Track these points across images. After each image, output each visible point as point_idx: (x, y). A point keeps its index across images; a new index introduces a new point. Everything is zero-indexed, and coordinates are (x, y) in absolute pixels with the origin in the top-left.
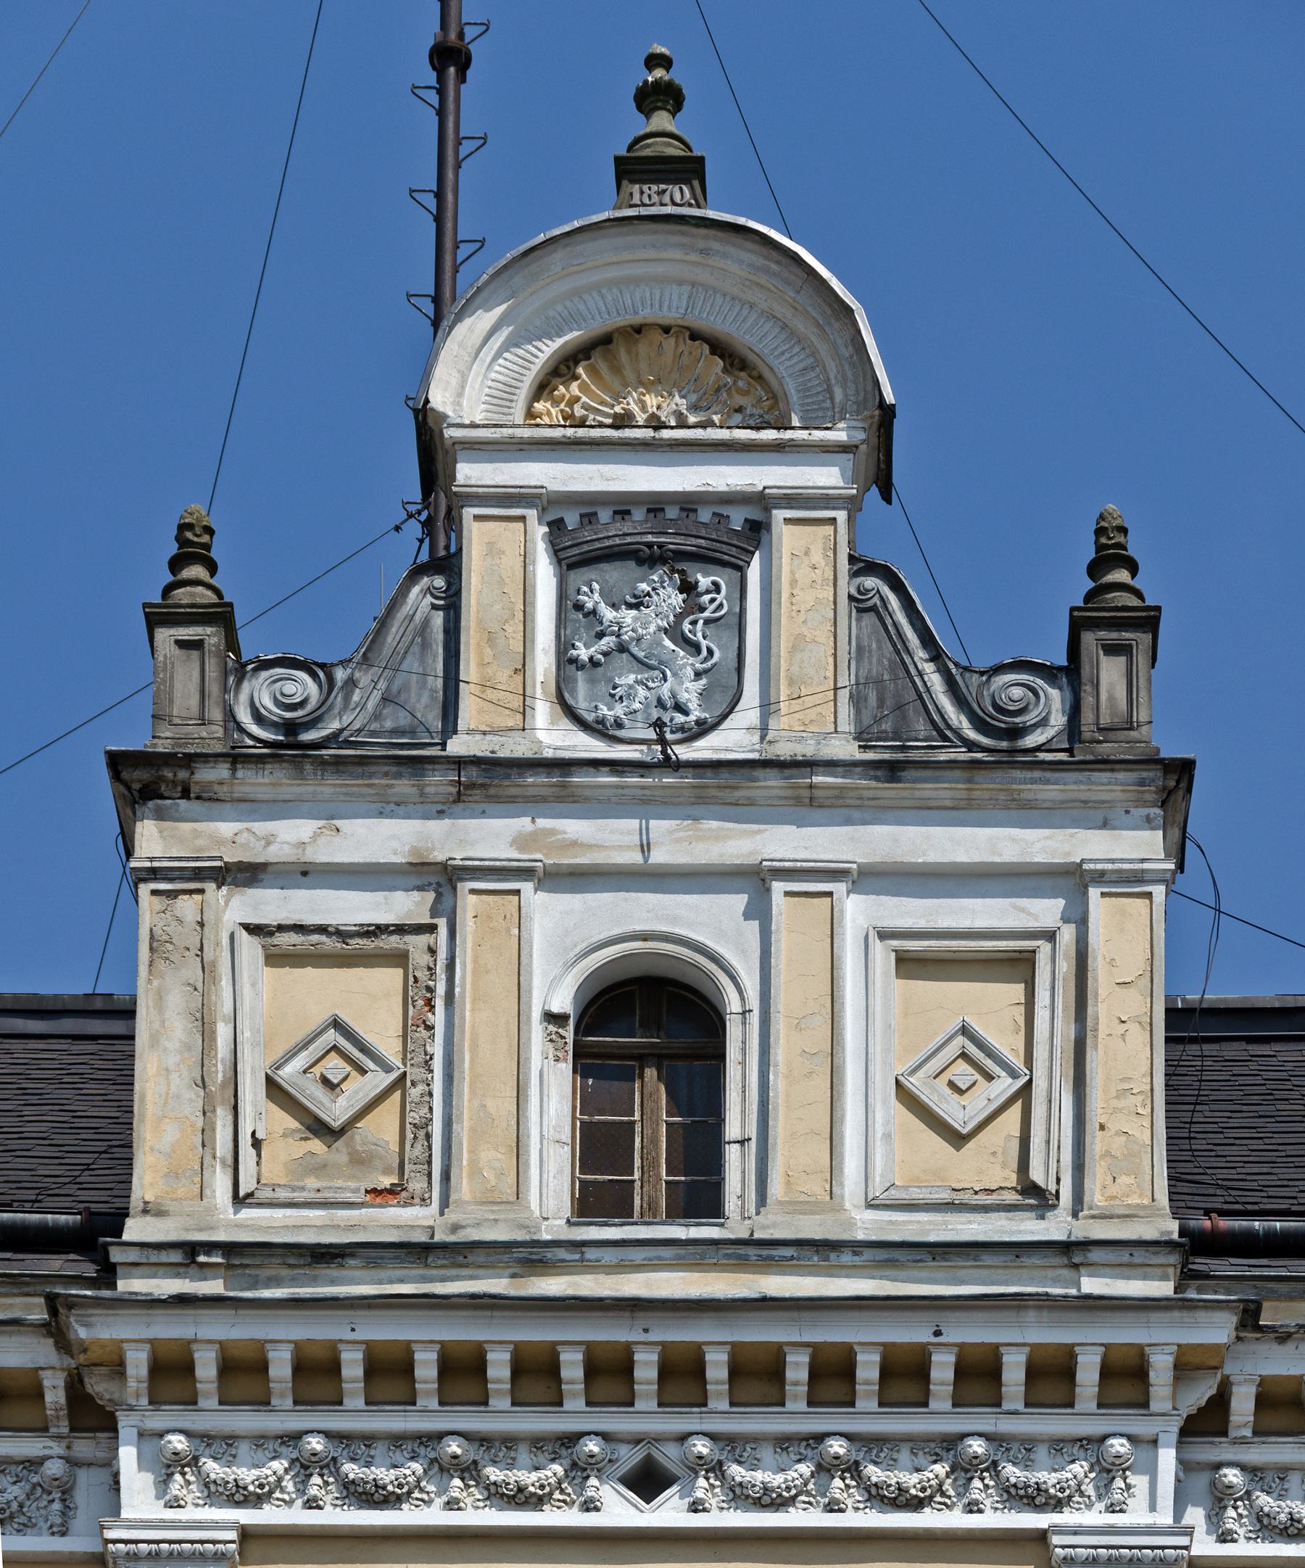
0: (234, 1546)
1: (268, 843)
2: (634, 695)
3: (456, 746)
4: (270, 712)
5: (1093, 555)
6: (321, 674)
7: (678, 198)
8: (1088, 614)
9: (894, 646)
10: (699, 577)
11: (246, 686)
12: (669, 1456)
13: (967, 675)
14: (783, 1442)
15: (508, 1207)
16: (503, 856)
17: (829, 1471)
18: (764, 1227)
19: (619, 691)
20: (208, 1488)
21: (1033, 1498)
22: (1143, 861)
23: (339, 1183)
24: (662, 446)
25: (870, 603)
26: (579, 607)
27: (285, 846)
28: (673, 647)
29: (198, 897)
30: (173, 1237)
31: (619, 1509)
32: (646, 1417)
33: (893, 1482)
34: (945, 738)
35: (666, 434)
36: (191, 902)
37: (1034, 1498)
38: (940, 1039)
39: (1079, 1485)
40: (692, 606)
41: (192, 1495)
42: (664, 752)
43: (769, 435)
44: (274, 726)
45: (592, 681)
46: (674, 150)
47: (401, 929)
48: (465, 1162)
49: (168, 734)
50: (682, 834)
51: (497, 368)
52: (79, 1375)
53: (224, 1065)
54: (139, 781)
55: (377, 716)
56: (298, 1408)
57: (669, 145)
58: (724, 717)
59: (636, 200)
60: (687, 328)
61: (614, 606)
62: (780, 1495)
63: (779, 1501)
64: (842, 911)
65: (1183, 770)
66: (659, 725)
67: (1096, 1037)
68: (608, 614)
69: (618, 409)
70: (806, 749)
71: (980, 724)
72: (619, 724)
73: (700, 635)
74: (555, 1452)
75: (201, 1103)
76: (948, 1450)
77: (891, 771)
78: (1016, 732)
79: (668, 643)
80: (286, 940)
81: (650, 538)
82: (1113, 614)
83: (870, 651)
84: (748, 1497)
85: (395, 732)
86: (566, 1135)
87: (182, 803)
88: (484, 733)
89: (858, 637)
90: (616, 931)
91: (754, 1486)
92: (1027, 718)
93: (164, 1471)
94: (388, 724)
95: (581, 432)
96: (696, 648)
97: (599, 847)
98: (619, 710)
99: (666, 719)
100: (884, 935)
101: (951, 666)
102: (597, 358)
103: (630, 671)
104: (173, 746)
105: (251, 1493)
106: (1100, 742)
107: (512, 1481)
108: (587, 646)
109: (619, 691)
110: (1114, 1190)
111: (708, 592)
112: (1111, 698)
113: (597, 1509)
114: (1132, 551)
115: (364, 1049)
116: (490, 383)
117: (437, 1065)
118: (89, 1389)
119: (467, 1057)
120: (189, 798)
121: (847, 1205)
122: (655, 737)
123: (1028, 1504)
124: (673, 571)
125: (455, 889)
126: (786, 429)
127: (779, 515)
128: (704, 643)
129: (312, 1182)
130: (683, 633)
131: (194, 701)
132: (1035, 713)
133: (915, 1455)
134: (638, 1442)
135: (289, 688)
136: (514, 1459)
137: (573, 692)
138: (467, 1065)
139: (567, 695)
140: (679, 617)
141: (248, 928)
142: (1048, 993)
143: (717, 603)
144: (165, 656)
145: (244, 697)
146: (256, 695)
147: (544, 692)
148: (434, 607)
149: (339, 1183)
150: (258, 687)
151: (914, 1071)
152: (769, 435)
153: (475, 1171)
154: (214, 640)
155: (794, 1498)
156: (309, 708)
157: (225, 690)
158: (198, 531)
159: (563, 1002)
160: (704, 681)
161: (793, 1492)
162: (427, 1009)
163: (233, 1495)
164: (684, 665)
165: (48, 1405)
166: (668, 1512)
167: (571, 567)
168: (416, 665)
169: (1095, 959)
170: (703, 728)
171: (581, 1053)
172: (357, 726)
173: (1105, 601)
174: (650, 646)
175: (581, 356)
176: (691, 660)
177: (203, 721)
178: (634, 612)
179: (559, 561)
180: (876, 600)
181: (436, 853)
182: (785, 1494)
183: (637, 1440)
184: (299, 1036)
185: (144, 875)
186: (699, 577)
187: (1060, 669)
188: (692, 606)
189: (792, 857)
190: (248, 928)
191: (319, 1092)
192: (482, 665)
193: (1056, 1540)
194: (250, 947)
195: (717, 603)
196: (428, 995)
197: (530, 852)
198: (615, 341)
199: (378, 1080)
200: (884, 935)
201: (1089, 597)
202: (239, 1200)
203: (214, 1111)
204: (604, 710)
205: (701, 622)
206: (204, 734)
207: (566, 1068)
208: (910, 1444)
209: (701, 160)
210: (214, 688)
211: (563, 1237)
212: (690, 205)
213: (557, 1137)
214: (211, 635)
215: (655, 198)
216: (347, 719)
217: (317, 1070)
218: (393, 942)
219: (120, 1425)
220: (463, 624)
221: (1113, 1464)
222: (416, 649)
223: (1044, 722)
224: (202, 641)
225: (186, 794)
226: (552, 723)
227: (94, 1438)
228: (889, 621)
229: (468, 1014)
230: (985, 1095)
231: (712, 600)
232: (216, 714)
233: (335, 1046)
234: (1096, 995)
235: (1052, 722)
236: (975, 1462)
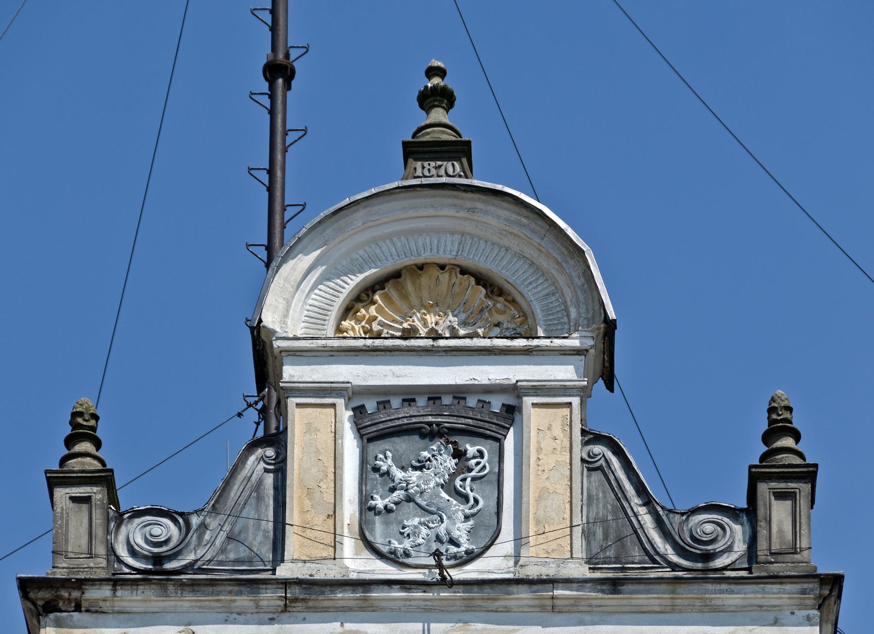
2: (418, 533)
4: (142, 548)
6: (181, 520)
7: (450, 171)
9: (616, 495)
10: (468, 446)
11: (123, 530)
19: (407, 531)
24: (439, 352)
25: (597, 464)
26: (376, 469)
28: (448, 498)
34: (654, 561)
40: (463, 468)
42: (441, 574)
43: (521, 343)
44: (145, 558)
51: (314, 296)
54: (43, 599)
55: (223, 550)
58: (487, 548)
59: (419, 172)
60: (458, 266)
61: (403, 468)
65: (835, 582)
68: (398, 474)
69: (406, 325)
70: (550, 571)
73: (468, 489)
77: (614, 585)
78: (708, 557)
79: (444, 495)
82: (781, 468)
83: (598, 499)
85: (237, 561)
87: (76, 615)
88: (305, 561)
89: (588, 489)
94: (232, 556)
101: (659, 509)
103: (415, 516)
104: (68, 574)
108: (382, 498)
111: (474, 457)
112: (780, 531)
116: (308, 307)
120: (80, 611)
126: (533, 338)
127: (528, 401)
128: (471, 495)
130: (455, 488)
131: (84, 541)
132: (723, 542)
135: (156, 530)
137: (372, 531)
139: (367, 534)
140: (453, 476)
143: (481, 465)
145: (122, 537)
146: (131, 536)
152: (521, 343)
156: (171, 545)
157: (108, 532)
158: (87, 417)
160: (471, 522)
167: (370, 440)
170: (471, 557)
172: (208, 557)
173: (775, 460)
174: (431, 497)
175: (377, 287)
176: (462, 507)
177: (91, 555)
178: (418, 473)
179: (361, 437)
180: (602, 462)
186: (468, 446)
188: (463, 468)
192: (303, 512)
195: (481, 465)
198: (403, 276)
204: (395, 544)
205: (469, 479)
206: (92, 565)
210: (99, 532)
212: (460, 176)
215: (434, 172)
216: (200, 552)
222: (252, 501)
223: (729, 549)
225: (78, 608)
226: (356, 554)
228: (612, 478)
232: (101, 550)
235: (736, 548)
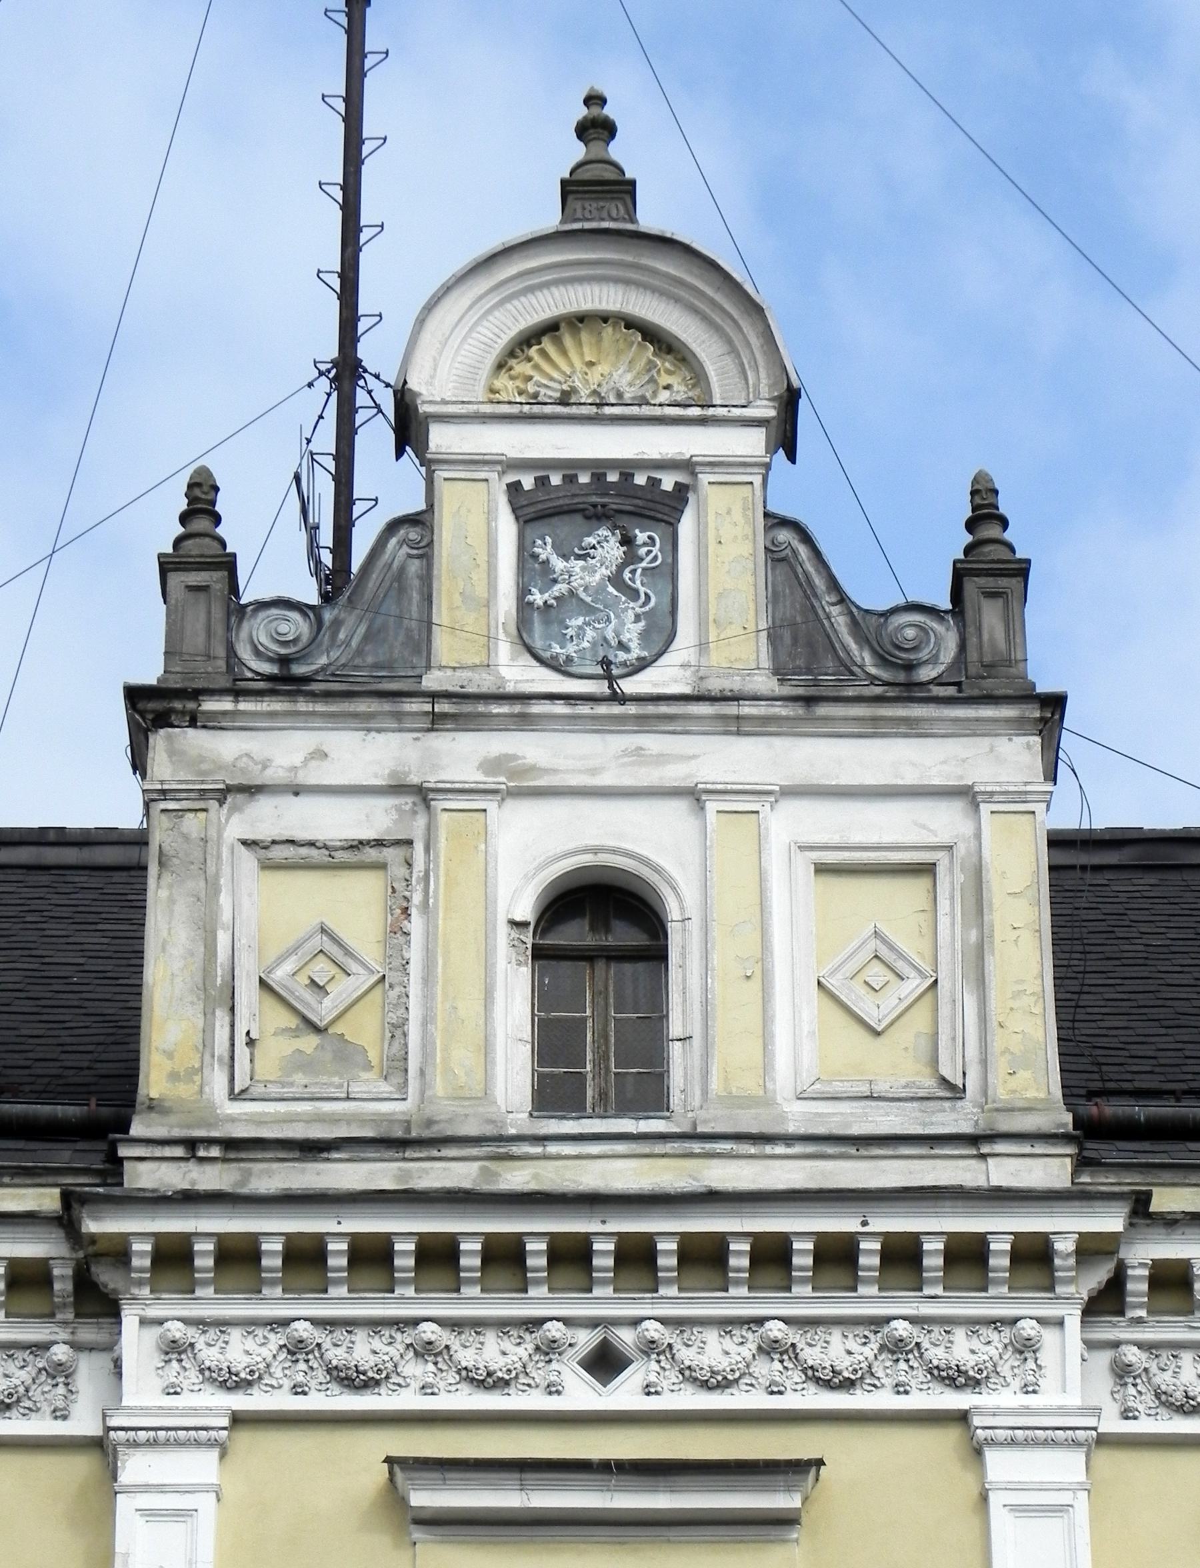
0: (226, 1433)
1: (265, 767)
2: (580, 637)
3: (431, 682)
4: (266, 648)
5: (970, 514)
6: (312, 616)
7: (614, 213)
8: (969, 566)
9: (805, 592)
10: (637, 531)
11: (246, 625)
12: (626, 1337)
13: (868, 617)
14: (726, 1324)
15: (477, 1102)
16: (472, 779)
17: (768, 1353)
18: (705, 1122)
19: (570, 632)
20: (203, 1374)
21: (955, 1378)
22: (1026, 783)
23: (325, 1079)
24: (603, 420)
25: (783, 554)
26: (535, 557)
27: (280, 770)
28: (616, 593)
29: (202, 815)
30: (177, 1133)
31: (581, 1393)
32: (604, 1302)
33: (827, 1365)
34: (852, 673)
35: (608, 410)
36: (196, 820)
37: (954, 1379)
38: (855, 943)
39: (995, 1366)
40: (631, 558)
41: (188, 1381)
42: (611, 686)
43: (695, 412)
44: (270, 660)
45: (547, 623)
46: (610, 175)
47: (379, 843)
48: (438, 1060)
49: (178, 669)
50: (626, 760)
51: (463, 352)
52: (87, 1263)
53: (223, 970)
54: (153, 711)
55: (359, 652)
56: (287, 1296)
57: (606, 170)
58: (660, 655)
59: (579, 215)
60: (623, 319)
61: (565, 557)
62: (725, 1378)
63: (724, 1382)
64: (767, 829)
65: (1056, 703)
66: (606, 663)
67: (992, 943)
68: (558, 564)
69: (565, 387)
70: (734, 684)
71: (883, 660)
72: (569, 660)
73: (638, 582)
74: (520, 1337)
75: (202, 1006)
76: (876, 1333)
77: (809, 701)
78: (910, 667)
79: (611, 589)
80: (278, 853)
81: (595, 499)
82: (990, 568)
83: (784, 596)
84: (696, 1379)
85: (376, 666)
86: (527, 1034)
87: (190, 731)
88: (454, 668)
89: (773, 585)
90: (571, 846)
91: (702, 1369)
92: (921, 655)
93: (163, 1357)
94: (370, 660)
95: (536, 409)
96: (633, 594)
97: (555, 771)
98: (571, 649)
99: (611, 658)
100: (802, 848)
101: (854, 610)
102: (547, 344)
103: (580, 614)
104: (183, 680)
105: (242, 1380)
106: (984, 678)
107: (481, 1366)
108: (541, 592)
109: (570, 632)
110: (1013, 1083)
111: (645, 544)
112: (992, 639)
113: (558, 1393)
114: (1003, 510)
115: (348, 952)
116: (457, 365)
117: (415, 969)
118: (94, 1278)
119: (440, 962)
120: (195, 727)
121: (779, 1100)
122: (602, 672)
123: (949, 1385)
124: (616, 527)
125: (428, 807)
126: (709, 406)
127: (704, 478)
128: (642, 590)
129: (300, 1078)
130: (624, 581)
131: (201, 640)
132: (926, 651)
133: (846, 1337)
134: (596, 1326)
135: (284, 628)
136: (482, 1343)
137: (530, 632)
138: (440, 970)
139: (525, 636)
140: (621, 568)
141: (244, 843)
142: (948, 902)
143: (652, 555)
144: (177, 600)
145: (244, 634)
146: (254, 633)
147: (505, 631)
148: (410, 556)
149: (325, 1079)
150: (256, 626)
151: (833, 972)
152: (695, 412)
153: (448, 1070)
154: (219, 586)
155: (737, 1381)
156: (300, 645)
157: (228, 629)
158: (205, 489)
159: (526, 910)
160: (642, 623)
161: (737, 1375)
162: (403, 917)
163: (225, 1381)
164: (626, 609)
165: (56, 1293)
166: (624, 1394)
167: (526, 522)
168: (394, 607)
169: (988, 871)
170: (642, 665)
171: (539, 954)
172: (343, 661)
173: (983, 554)
174: (597, 592)
175: (533, 341)
176: (632, 605)
177: (209, 657)
178: (581, 563)
179: (517, 518)
180: (788, 551)
181: (412, 776)
182: (730, 1377)
183: (593, 1323)
184: (290, 942)
185: (155, 796)
186: (637, 531)
187: (946, 612)
188: (631, 558)
189: (722, 780)
190: (244, 843)
191: (308, 996)
192: (451, 609)
193: (977, 1421)
194: (248, 860)
195: (652, 555)
196: (405, 904)
197: (495, 775)
198: (562, 330)
199: (361, 981)
200: (802, 848)
201: (968, 550)
202: (234, 1096)
203: (214, 1013)
204: (557, 649)
205: (639, 571)
206: (210, 670)
207: (526, 971)
208: (842, 1327)
209: (633, 183)
210: (219, 629)
211: (528, 1131)
212: (624, 220)
213: (520, 1036)
214: (214, 579)
215: (595, 213)
216: (334, 654)
217: (307, 971)
218: (372, 854)
219: (123, 1314)
220: (435, 572)
221: (1025, 1346)
222: (393, 593)
223: (934, 660)
224: (208, 586)
225: (193, 724)
226: (512, 659)
227: (97, 1323)
228: (799, 570)
229: (440, 922)
230: (896, 995)
231: (650, 552)
232: (221, 651)
233: (321, 951)
234: (991, 904)
235: (942, 659)
236: (900, 1344)
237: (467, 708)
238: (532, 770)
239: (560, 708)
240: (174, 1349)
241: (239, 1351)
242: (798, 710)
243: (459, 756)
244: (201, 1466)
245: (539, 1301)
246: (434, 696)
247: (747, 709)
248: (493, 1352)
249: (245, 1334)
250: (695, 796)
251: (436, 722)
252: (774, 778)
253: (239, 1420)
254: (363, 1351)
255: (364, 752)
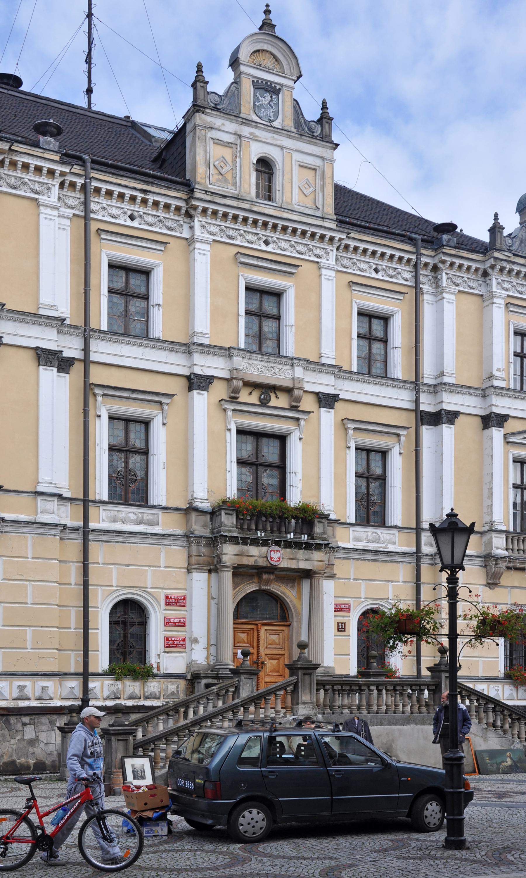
237: (248, 122)
238: (256, 136)
239: (262, 126)
240: (203, 226)
241: (212, 229)
242: (299, 136)
243: (246, 131)
244: (207, 247)
245: (258, 231)
246: (243, 119)
247: (292, 134)
248: (250, 237)
249: (215, 226)
250: (282, 148)
251: (243, 123)
252: (294, 148)
253: (214, 241)
254: (231, 233)
255: (231, 126)
